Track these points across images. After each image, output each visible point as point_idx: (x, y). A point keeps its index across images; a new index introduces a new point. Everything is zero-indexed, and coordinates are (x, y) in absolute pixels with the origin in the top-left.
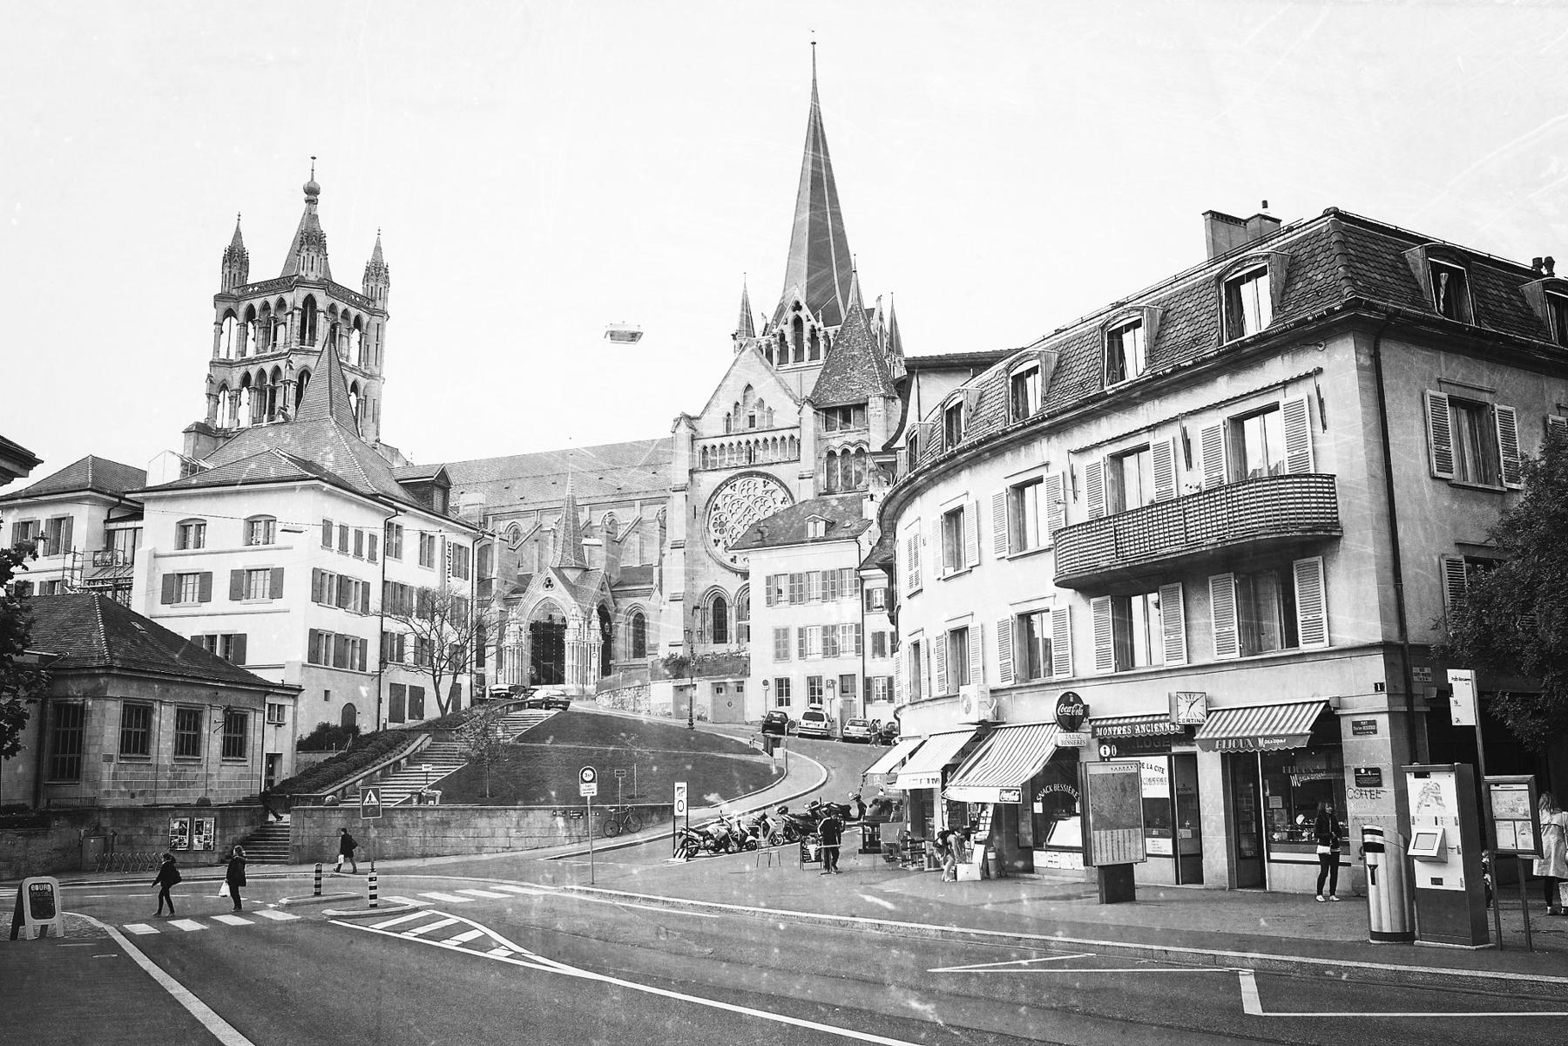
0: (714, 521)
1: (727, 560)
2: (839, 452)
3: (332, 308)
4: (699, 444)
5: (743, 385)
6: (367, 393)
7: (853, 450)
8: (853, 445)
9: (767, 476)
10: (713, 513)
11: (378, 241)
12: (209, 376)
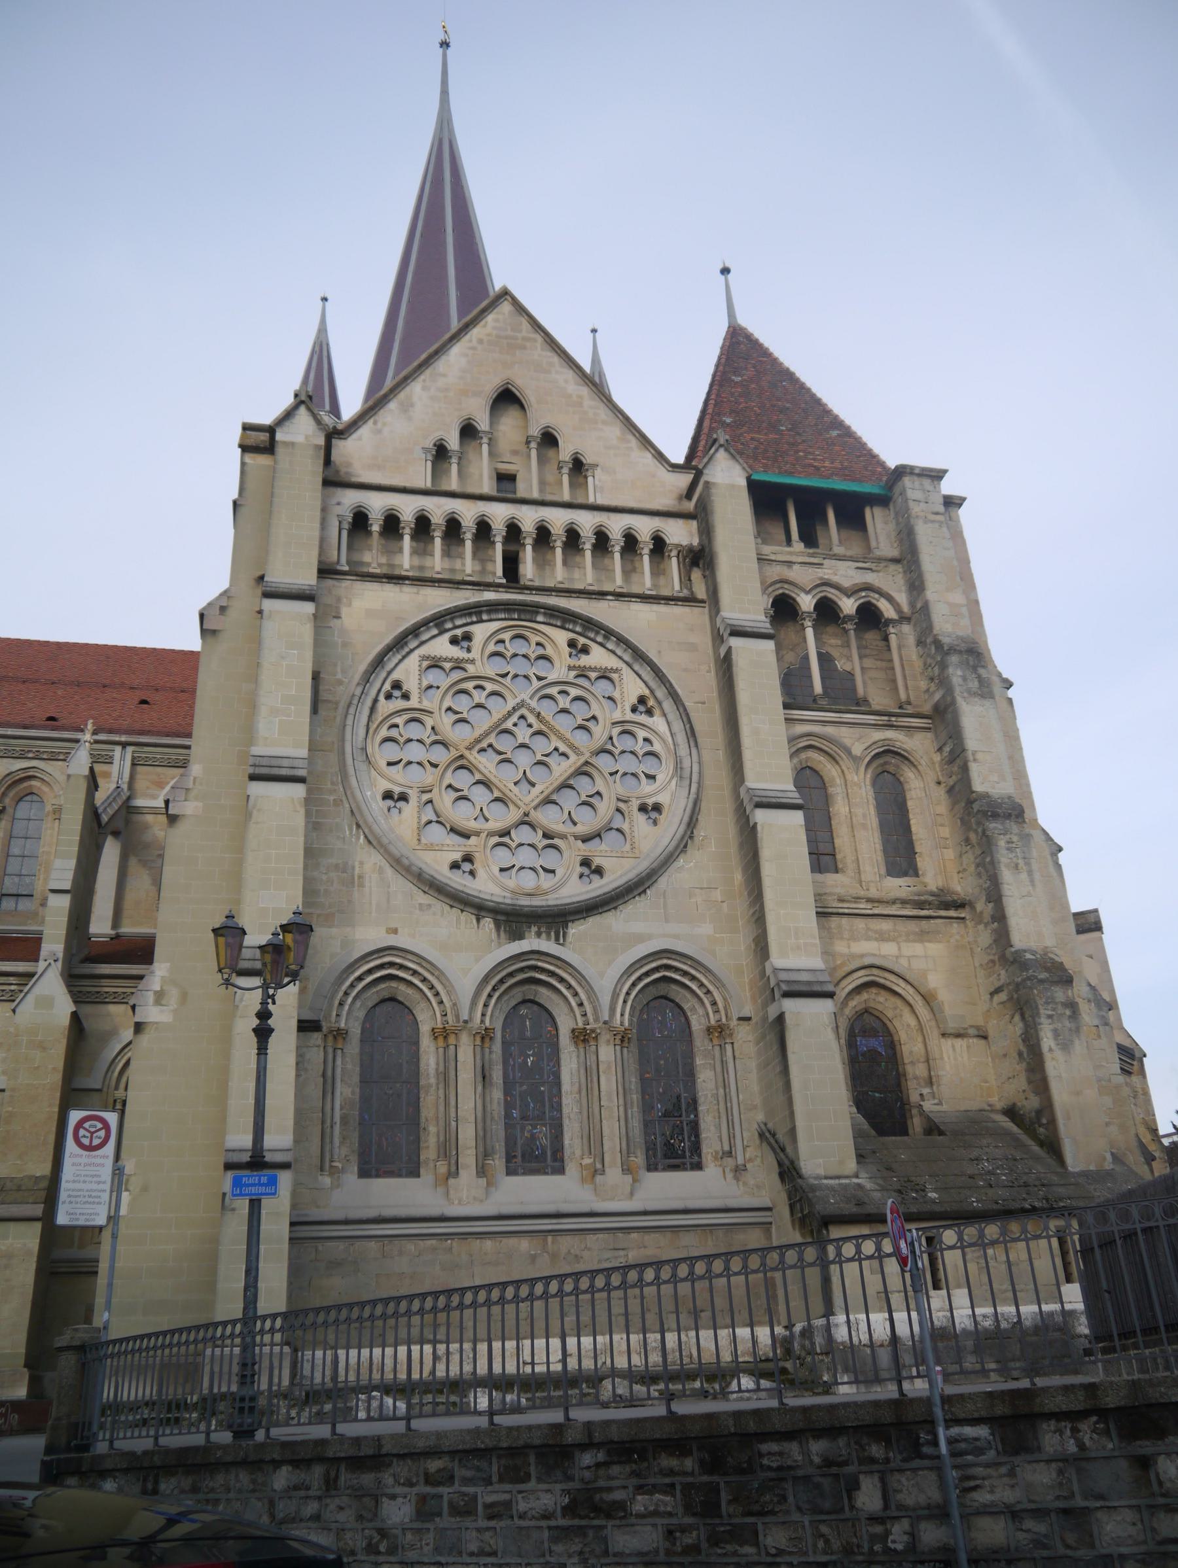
0: (384, 732)
1: (438, 864)
2: (806, 603)
4: (350, 499)
5: (491, 385)
7: (848, 606)
8: (849, 593)
9: (590, 625)
10: (385, 707)
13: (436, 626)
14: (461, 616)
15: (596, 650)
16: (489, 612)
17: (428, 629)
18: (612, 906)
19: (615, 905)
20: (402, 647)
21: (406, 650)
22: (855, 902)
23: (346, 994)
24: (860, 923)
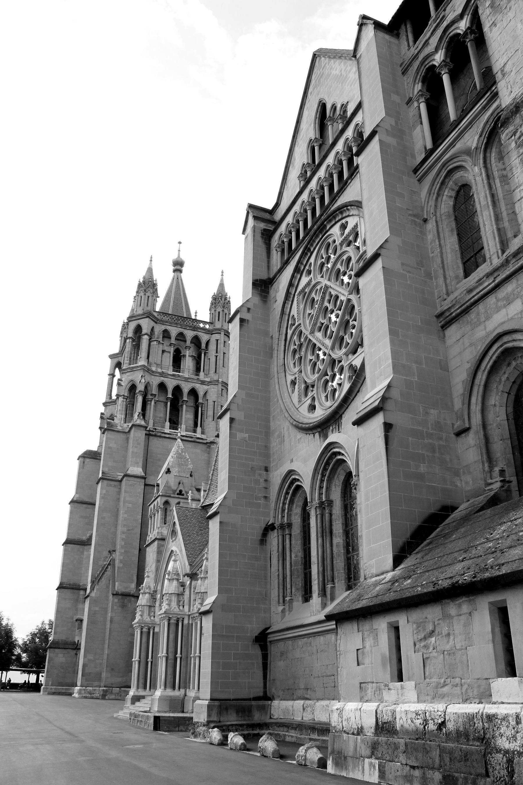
3: (166, 334)
6: (208, 397)
11: (222, 280)
12: (102, 414)
13: (298, 272)
14: (304, 258)
15: (349, 219)
16: (312, 245)
17: (296, 278)
18: (356, 392)
19: (357, 390)
20: (290, 297)
21: (292, 296)
22: (481, 284)
23: (284, 504)
24: (491, 300)
